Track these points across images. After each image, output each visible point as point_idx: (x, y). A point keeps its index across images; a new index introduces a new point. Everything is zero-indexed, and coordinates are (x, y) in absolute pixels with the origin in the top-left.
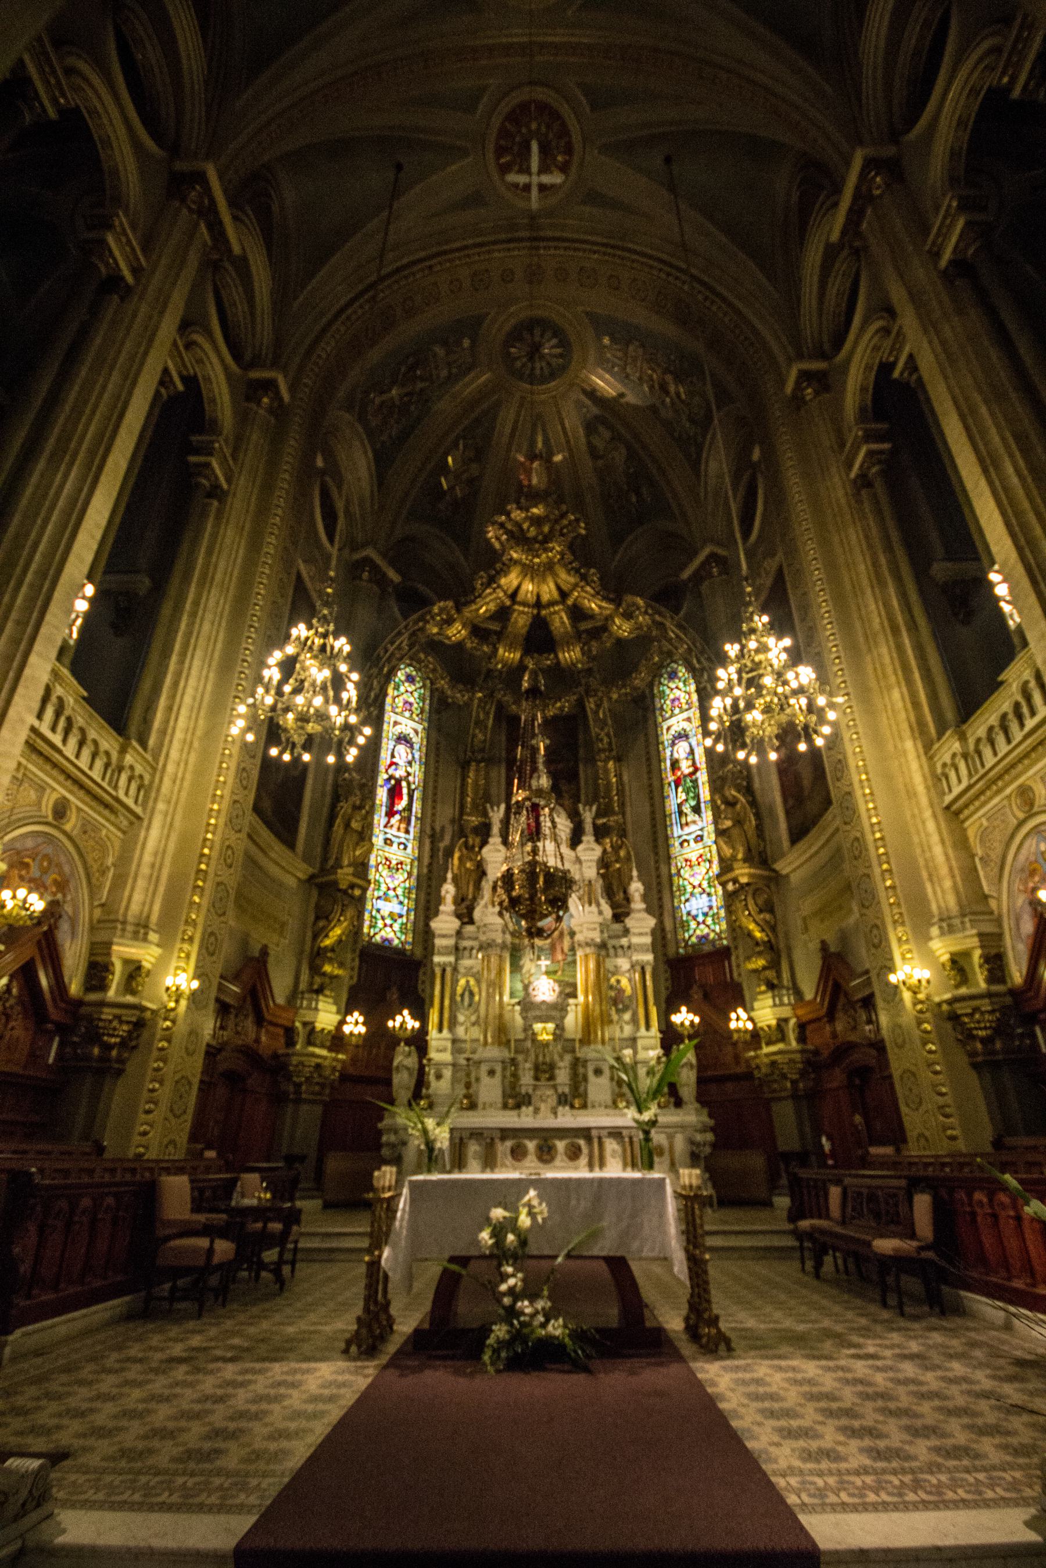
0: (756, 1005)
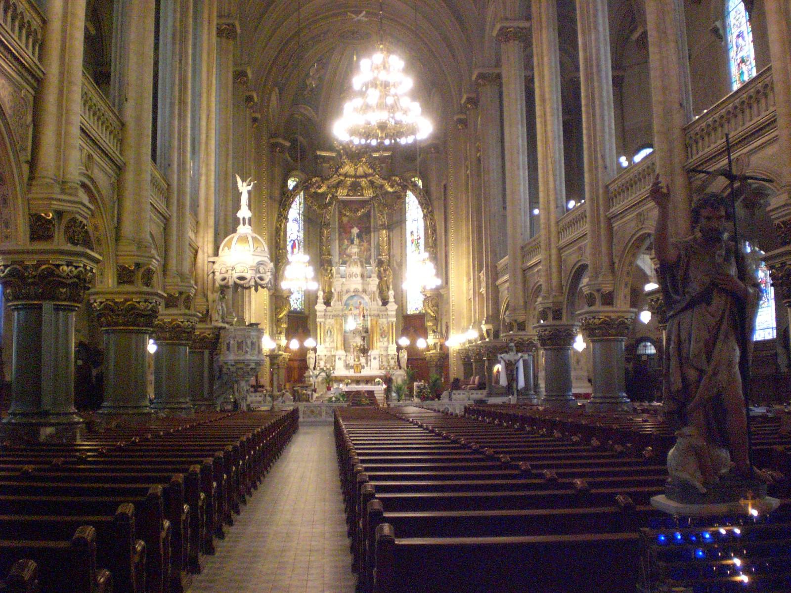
0: (429, 337)
